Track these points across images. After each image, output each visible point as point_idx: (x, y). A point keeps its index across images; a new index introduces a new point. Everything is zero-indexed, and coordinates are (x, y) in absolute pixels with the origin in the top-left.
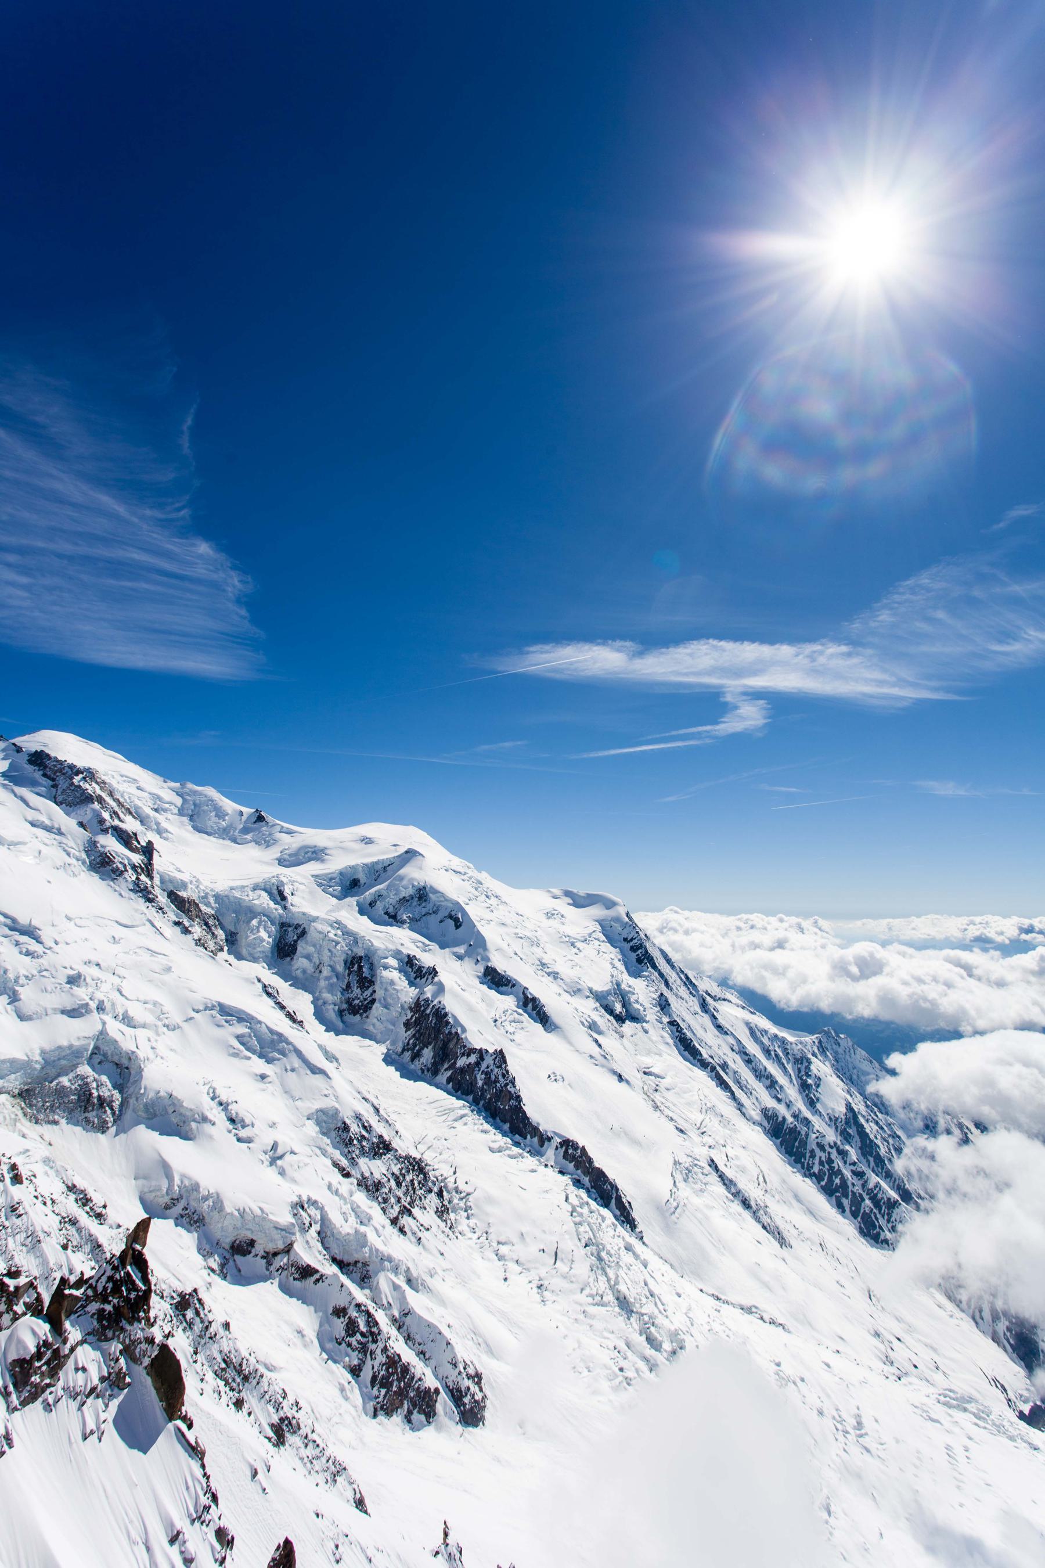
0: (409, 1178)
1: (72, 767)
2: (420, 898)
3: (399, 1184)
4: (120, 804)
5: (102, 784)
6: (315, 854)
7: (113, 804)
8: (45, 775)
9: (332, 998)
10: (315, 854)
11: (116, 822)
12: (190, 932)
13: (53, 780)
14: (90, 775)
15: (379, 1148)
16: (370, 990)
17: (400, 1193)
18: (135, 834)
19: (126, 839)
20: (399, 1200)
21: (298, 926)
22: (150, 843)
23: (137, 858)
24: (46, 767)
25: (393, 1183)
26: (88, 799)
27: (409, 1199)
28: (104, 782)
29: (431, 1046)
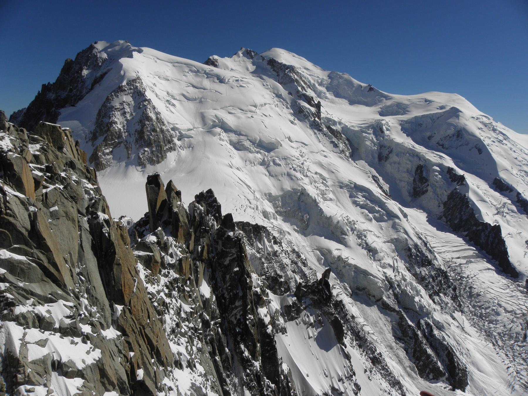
0: (439, 279)
1: (285, 65)
2: (458, 136)
3: (434, 280)
4: (305, 83)
5: (297, 73)
6: (399, 109)
7: (302, 83)
8: (274, 70)
9: (405, 188)
10: (399, 109)
11: (304, 92)
12: (338, 147)
13: (277, 72)
14: (291, 68)
15: (425, 262)
16: (426, 184)
17: (433, 284)
18: (312, 98)
19: (309, 100)
20: (433, 287)
21: (389, 147)
22: (319, 102)
23: (313, 110)
24: (274, 66)
25: (431, 280)
26: (292, 81)
27: (438, 288)
28: (298, 72)
29: (458, 217)
